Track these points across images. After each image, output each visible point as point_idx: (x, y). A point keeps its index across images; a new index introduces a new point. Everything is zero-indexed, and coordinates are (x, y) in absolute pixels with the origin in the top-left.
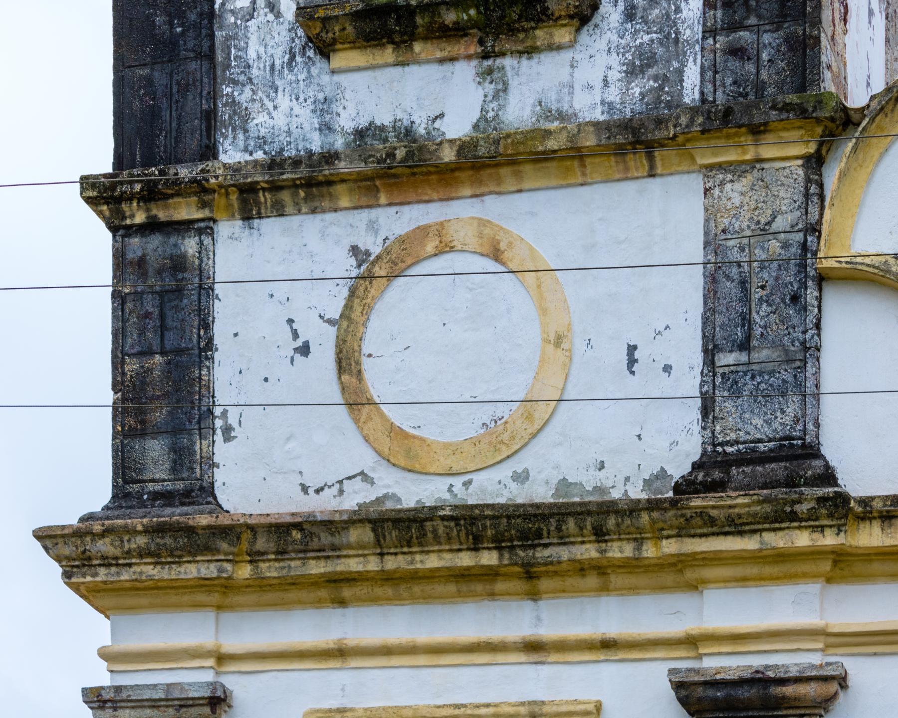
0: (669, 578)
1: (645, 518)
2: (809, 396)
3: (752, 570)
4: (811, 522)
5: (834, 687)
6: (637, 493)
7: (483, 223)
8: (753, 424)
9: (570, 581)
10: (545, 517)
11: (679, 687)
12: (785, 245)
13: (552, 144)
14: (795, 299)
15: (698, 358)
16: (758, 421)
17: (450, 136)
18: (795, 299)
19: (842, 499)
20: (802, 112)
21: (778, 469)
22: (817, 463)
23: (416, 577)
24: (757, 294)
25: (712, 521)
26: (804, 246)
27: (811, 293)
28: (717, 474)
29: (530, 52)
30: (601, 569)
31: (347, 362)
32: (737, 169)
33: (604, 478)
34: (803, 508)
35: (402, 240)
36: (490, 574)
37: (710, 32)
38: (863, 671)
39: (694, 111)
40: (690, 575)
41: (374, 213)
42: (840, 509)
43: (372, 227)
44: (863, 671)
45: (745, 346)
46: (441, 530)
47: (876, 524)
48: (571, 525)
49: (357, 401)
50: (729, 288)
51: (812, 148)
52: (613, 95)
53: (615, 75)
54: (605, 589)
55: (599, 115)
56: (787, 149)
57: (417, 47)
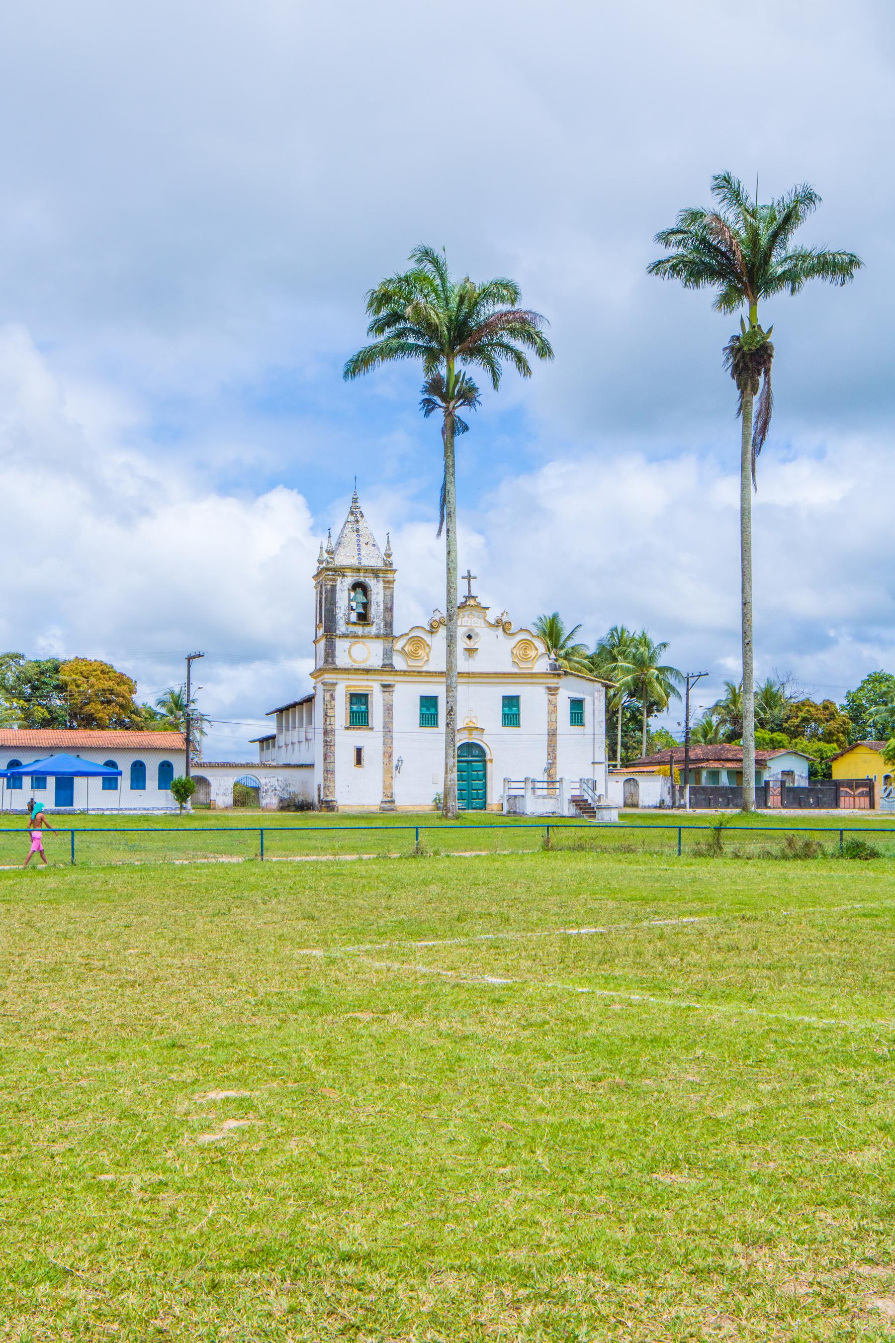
8: (387, 662)
31: (349, 653)
49: (350, 656)
56: (391, 639)
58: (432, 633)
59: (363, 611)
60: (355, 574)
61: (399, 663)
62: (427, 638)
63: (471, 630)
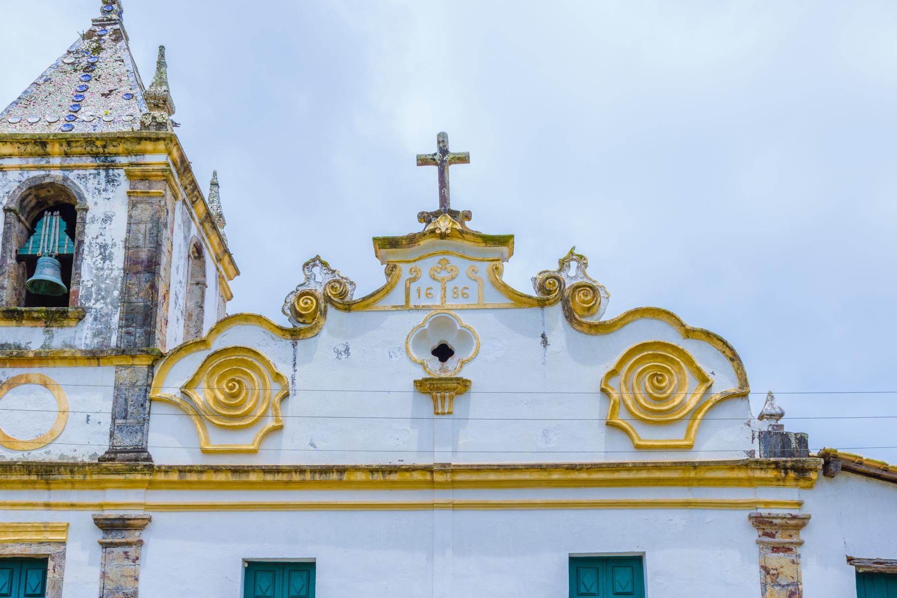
0: (95, 486)
1: (87, 468)
2: (145, 434)
3: (123, 485)
4: (142, 472)
5: (146, 522)
6: (87, 460)
7: (41, 375)
8: (126, 441)
9: (61, 486)
10: (53, 466)
11: (95, 520)
12: (140, 390)
13: (66, 355)
14: (142, 405)
15: (110, 420)
16: (128, 440)
17: (33, 349)
18: (142, 405)
19: (153, 466)
20: (147, 353)
21: (132, 455)
22: (146, 454)
23: (8, 482)
24: (130, 403)
25: (109, 470)
26: (146, 390)
27: (147, 404)
28: (113, 456)
29: (62, 327)
30: (72, 483)
32: (127, 367)
33: (76, 454)
34: (139, 468)
35: (13, 378)
36: (34, 483)
37: (120, 327)
38: (156, 516)
39: (113, 350)
40: (102, 485)
41: (4, 370)
42: (151, 468)
43: (4, 374)
44: (156, 516)
45: (125, 418)
46: (17, 468)
47: (163, 474)
48: (62, 469)
50: (121, 401)
51: (150, 363)
52: (88, 342)
53: (89, 336)
54: (73, 488)
55: (83, 348)
56: (142, 362)
57: (24, 322)
58: (294, 334)
59: (59, 281)
60: (31, 162)
61: (169, 441)
62: (276, 352)
63: (443, 322)
